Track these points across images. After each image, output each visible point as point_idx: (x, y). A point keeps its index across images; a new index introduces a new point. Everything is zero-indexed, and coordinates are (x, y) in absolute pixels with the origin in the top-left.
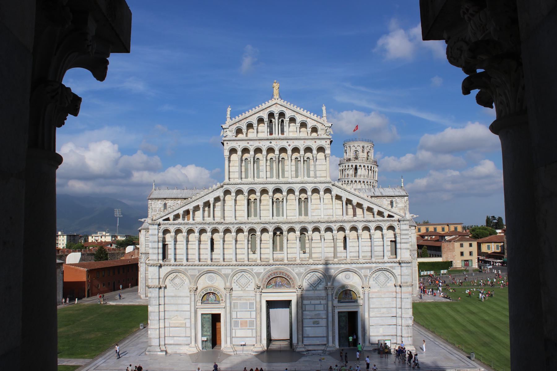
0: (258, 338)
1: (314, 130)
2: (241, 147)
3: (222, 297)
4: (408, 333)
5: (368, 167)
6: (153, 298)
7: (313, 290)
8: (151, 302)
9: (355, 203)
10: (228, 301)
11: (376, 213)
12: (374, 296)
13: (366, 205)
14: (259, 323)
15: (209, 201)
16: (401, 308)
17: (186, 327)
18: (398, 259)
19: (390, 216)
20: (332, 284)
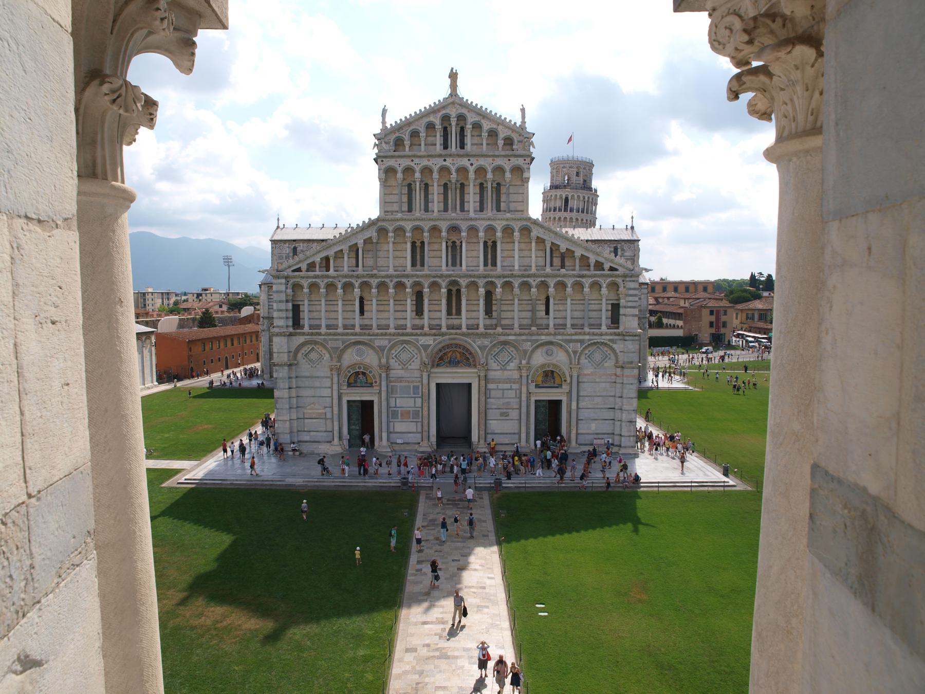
0: (425, 434)
1: (509, 142)
3: (375, 378)
4: (630, 431)
5: (584, 198)
9: (563, 249)
10: (384, 384)
11: (592, 265)
12: (585, 380)
13: (578, 253)
14: (425, 413)
15: (356, 244)
17: (326, 419)
20: (528, 363)
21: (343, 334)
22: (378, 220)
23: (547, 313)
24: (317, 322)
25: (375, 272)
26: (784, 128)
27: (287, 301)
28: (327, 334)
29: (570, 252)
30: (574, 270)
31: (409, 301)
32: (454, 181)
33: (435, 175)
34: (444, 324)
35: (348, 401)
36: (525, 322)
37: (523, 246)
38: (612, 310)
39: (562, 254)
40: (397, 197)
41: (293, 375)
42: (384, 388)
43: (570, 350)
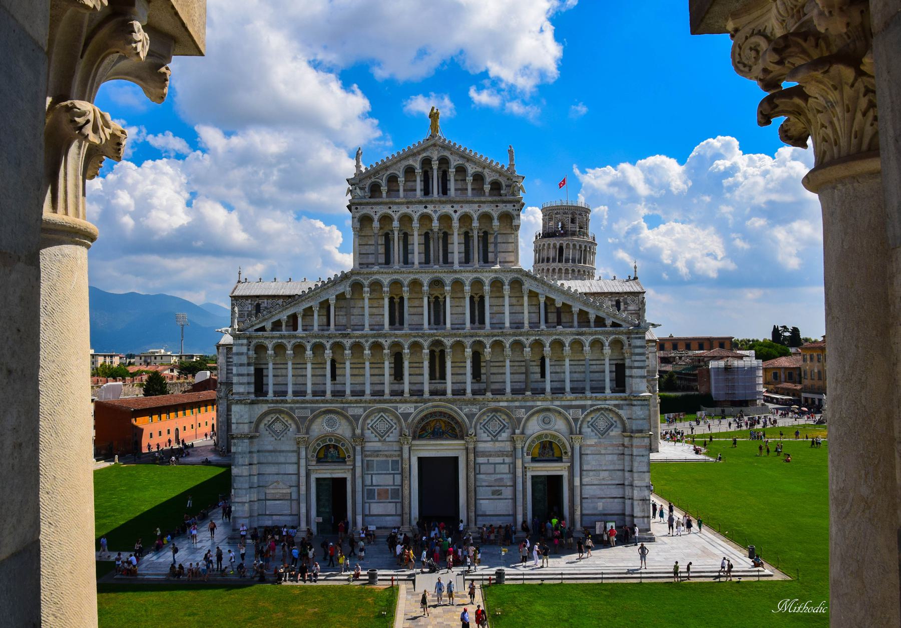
1: (496, 187)
2: (378, 214)
4: (643, 511)
5: (580, 246)
6: (240, 453)
7: (492, 440)
8: (236, 460)
10: (358, 458)
12: (589, 452)
16: (631, 471)
17: (291, 500)
18: (628, 391)
19: (614, 325)
21: (312, 402)
22: (352, 273)
23: (543, 375)
24: (283, 388)
25: (349, 331)
26: (825, 152)
27: (249, 364)
28: (294, 402)
29: (567, 307)
30: (571, 327)
31: (387, 364)
32: (436, 229)
33: (416, 224)
34: (426, 388)
35: (318, 480)
36: (517, 386)
37: (514, 301)
38: (616, 371)
39: (558, 309)
40: (373, 248)
41: (255, 449)
42: (358, 464)
43: (570, 418)
